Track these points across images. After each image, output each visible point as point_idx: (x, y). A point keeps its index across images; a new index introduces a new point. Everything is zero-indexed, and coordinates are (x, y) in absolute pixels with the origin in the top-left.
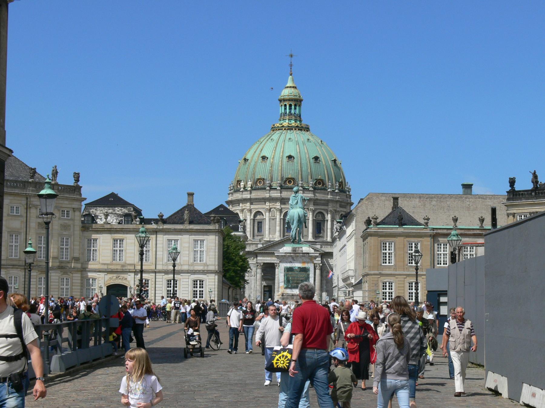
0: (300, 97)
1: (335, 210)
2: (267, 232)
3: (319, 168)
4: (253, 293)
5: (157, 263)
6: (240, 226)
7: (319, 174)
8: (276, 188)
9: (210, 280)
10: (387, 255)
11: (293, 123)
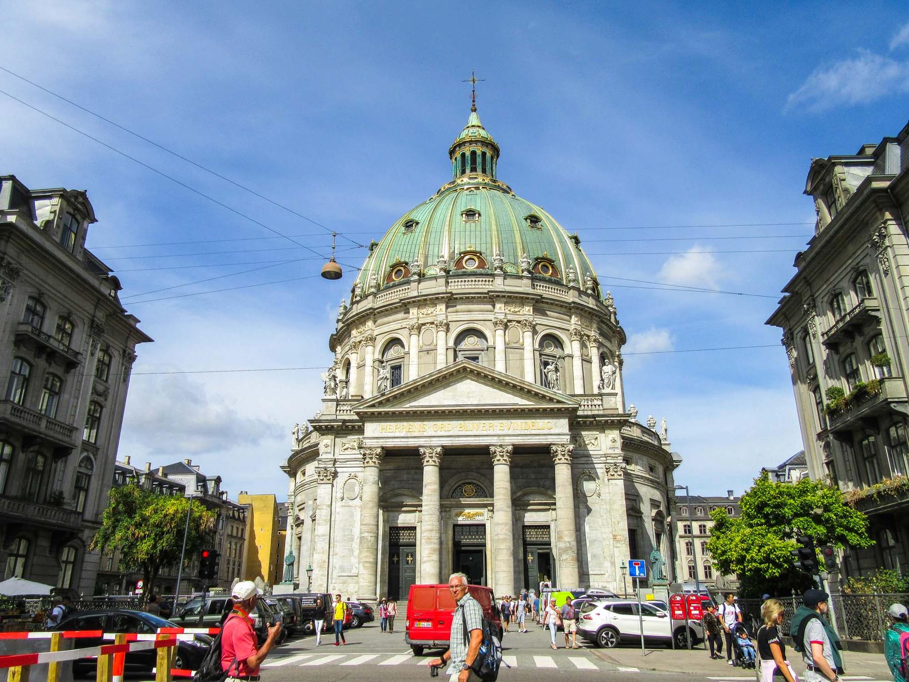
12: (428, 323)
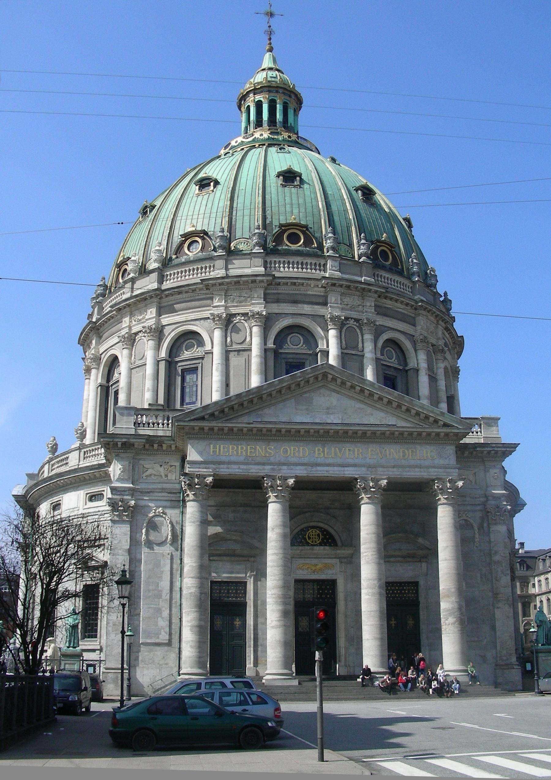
1: (433, 345)
12: (239, 314)
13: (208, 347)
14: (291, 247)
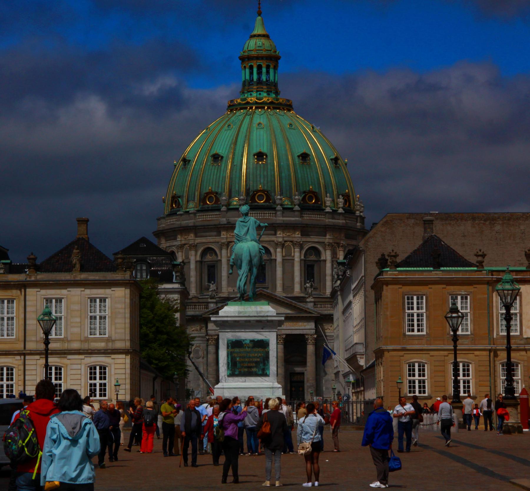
0: (275, 52)
2: (224, 283)
3: (309, 173)
4: (202, 386)
5: (27, 339)
6: (174, 273)
7: (310, 183)
8: (237, 209)
9: (117, 366)
10: (415, 318)
11: (265, 97)
13: (219, 258)
14: (258, 203)
